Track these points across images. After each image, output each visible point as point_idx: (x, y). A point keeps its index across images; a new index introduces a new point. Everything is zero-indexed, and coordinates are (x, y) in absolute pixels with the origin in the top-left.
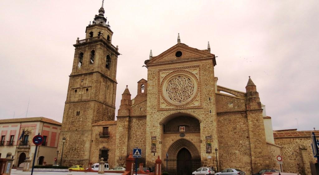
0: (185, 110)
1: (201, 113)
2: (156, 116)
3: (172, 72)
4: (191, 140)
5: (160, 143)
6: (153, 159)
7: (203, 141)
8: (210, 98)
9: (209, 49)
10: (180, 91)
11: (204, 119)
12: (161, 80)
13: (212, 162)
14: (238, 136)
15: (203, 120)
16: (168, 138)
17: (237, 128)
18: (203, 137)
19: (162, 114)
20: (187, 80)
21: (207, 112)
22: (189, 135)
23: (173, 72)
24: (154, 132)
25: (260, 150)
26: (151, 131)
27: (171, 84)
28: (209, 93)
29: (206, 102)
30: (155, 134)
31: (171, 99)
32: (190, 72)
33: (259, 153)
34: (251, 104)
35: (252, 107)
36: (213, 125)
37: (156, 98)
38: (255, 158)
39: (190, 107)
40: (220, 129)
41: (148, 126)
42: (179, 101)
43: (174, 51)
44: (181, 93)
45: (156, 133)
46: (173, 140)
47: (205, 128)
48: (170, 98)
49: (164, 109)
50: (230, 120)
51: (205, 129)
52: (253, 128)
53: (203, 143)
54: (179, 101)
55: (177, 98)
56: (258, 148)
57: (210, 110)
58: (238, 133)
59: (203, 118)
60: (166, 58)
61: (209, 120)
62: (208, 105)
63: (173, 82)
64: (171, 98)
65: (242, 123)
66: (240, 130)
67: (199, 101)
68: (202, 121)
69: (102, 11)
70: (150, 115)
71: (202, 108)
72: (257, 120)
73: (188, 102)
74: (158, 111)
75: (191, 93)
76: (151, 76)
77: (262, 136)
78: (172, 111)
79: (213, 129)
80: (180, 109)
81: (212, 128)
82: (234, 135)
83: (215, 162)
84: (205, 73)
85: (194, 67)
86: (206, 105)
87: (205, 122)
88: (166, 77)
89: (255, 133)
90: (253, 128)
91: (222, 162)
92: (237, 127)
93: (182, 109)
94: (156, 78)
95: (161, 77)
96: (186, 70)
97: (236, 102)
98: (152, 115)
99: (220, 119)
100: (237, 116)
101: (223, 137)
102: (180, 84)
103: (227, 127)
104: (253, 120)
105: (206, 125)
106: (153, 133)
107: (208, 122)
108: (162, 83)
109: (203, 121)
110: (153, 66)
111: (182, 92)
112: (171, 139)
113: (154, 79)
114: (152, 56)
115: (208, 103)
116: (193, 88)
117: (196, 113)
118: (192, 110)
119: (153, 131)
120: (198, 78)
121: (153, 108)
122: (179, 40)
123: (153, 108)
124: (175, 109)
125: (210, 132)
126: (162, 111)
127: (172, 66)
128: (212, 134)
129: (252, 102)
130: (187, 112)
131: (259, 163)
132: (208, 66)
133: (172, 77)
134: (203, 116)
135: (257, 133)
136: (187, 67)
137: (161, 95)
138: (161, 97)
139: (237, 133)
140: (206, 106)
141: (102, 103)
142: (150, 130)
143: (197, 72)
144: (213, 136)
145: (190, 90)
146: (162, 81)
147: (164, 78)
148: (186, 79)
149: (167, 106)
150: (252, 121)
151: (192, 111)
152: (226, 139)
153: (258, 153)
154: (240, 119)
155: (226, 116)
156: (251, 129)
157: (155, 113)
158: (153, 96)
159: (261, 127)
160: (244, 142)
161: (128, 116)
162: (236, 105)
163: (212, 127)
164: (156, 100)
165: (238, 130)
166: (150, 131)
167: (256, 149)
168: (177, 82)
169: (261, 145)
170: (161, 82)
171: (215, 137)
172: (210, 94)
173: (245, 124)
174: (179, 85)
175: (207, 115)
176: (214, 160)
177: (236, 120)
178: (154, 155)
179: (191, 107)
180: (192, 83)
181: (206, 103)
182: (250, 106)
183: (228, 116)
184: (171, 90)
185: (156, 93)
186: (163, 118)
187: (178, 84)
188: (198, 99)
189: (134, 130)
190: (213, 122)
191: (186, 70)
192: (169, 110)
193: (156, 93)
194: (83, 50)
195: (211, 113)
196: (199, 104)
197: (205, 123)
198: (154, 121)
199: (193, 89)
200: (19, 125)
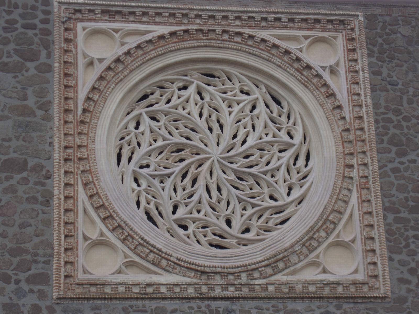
3: (162, 37)
10: (217, 171)
20: (261, 107)
23: (173, 34)
27: (153, 118)
29: (404, 257)
31: (150, 218)
32: (287, 52)
39: (299, 288)
42: (211, 237)
48: (147, 214)
49: (108, 290)
54: (211, 237)
55: (195, 215)
63: (162, 106)
64: (155, 213)
67: (358, 246)
73: (280, 247)
75: (296, 194)
80: (232, 291)
84: (385, 72)
85: (317, 21)
86: (407, 276)
88: (118, 60)
93: (245, 291)
95: (81, 62)
102: (216, 126)
108: (88, 99)
111: (233, 177)
116: (301, 162)
123: (22, 276)
124: (191, 291)
136: (271, 17)
137: (85, 185)
138: (82, 195)
140: (404, 287)
143: (332, 62)
145: (283, 169)
146: (94, 89)
147: (109, 68)
148: (256, 94)
149: (130, 264)
158: (21, 189)
170: (82, 94)
174: (211, 129)
179: (307, 283)
180: (300, 128)
181: (402, 263)
184: (153, 161)
187: (202, 124)
188: (347, 239)
196: (356, 271)
199: (304, 171)
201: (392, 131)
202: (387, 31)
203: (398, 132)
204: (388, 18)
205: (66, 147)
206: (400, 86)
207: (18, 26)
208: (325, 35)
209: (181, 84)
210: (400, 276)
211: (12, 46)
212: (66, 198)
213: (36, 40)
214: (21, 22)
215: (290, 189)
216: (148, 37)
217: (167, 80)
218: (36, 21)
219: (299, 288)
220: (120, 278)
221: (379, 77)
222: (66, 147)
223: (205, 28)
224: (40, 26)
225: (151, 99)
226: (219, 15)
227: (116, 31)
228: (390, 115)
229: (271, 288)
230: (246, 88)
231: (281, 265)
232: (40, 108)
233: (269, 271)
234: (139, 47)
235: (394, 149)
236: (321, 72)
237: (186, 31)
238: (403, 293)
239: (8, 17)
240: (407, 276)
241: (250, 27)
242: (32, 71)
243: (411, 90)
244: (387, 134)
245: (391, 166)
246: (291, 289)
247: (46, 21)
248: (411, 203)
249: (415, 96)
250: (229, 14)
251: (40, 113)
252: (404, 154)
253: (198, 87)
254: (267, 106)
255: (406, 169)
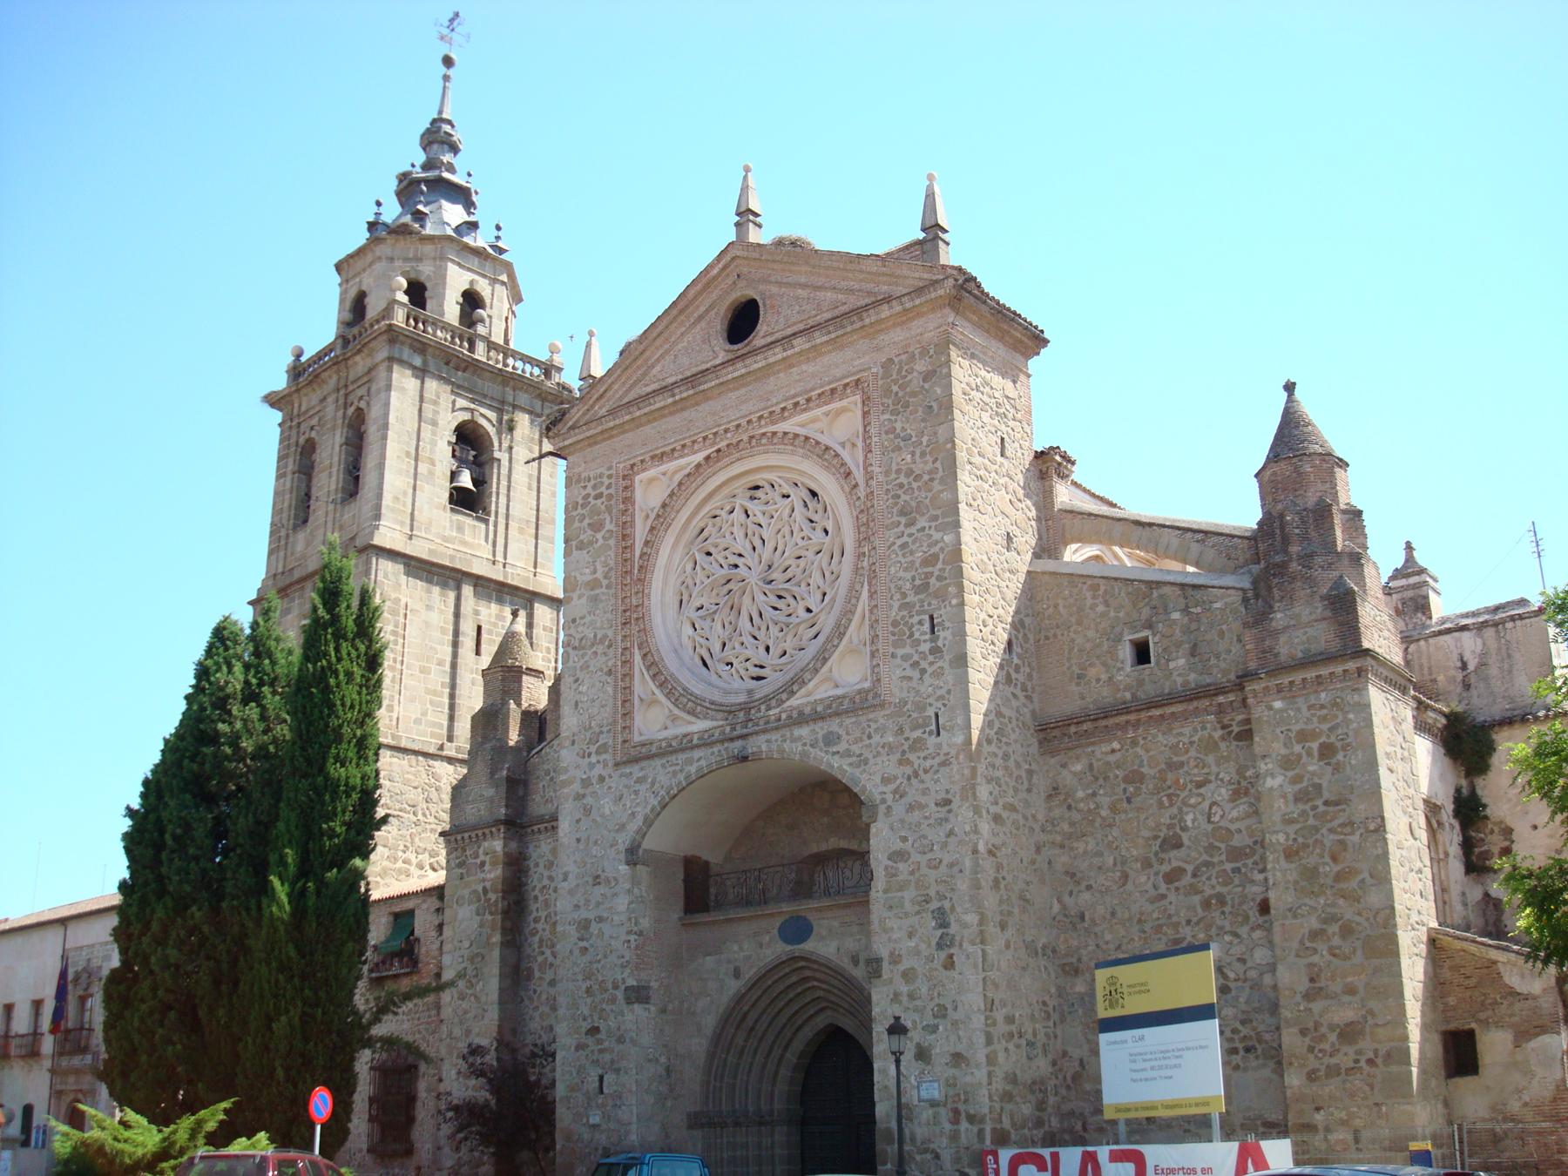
0: (774, 736)
1: (876, 738)
2: (607, 806)
3: (699, 466)
4: (846, 964)
5: (629, 1002)
6: (592, 1121)
7: (885, 965)
8: (932, 618)
9: (933, 231)
11: (892, 787)
12: (640, 532)
13: (948, 1127)
14: (1196, 899)
15: (889, 797)
16: (709, 961)
17: (1185, 837)
18: (885, 931)
19: (643, 788)
21: (917, 734)
22: (836, 924)
23: (708, 458)
24: (600, 919)
25: (1344, 1014)
26: (584, 914)
28: (928, 575)
30: (601, 934)
31: (705, 664)
33: (1340, 1035)
34: (1279, 618)
35: (1283, 639)
36: (951, 833)
37: (610, 673)
38: (1312, 1076)
40: (1064, 859)
41: (565, 879)
43: (711, 307)
44: (769, 613)
45: (607, 929)
46: (737, 974)
47: (898, 856)
50: (1135, 778)
51: (901, 866)
52: (1292, 821)
53: (891, 981)
56: (1337, 987)
57: (931, 712)
58: (1194, 875)
59: (886, 780)
60: (668, 369)
61: (925, 792)
62: (923, 671)
65: (1224, 793)
66: (1211, 849)
68: (882, 808)
69: (437, 138)
70: (579, 797)
71: (882, 706)
72: (1327, 751)
74: (617, 765)
76: (583, 517)
77: (1369, 881)
78: (697, 754)
79: (951, 865)
81: (947, 860)
82: (1163, 897)
83: (964, 1125)
84: (898, 426)
85: (833, 391)
86: (909, 672)
87: (899, 809)
88: (664, 506)
89: (1311, 861)
90: (1292, 821)
91: (1079, 1127)
92: (1184, 829)
94: (609, 526)
96: (782, 427)
97: (1176, 616)
98: (589, 800)
99: (1067, 778)
100: (1187, 731)
101: (1082, 917)
103: (1115, 832)
104: (1299, 756)
105: (904, 839)
106: (594, 928)
107: (921, 807)
108: (643, 555)
109: (889, 808)
110: (592, 441)
112: (729, 962)
113: (599, 536)
114: (590, 376)
115: (923, 655)
117: (842, 747)
118: (821, 729)
119: (591, 916)
120: (859, 475)
121: (593, 749)
122: (746, 216)
125: (932, 893)
126: (644, 763)
127: (702, 417)
128: (947, 904)
129: (1290, 598)
130: (786, 746)
131: (1344, 1123)
132: (921, 366)
133: (710, 495)
134: (888, 764)
135: (1327, 859)
138: (638, 658)
139: (1187, 880)
141: (426, 755)
142: (577, 907)
144: (952, 919)
145: (817, 576)
147: (658, 516)
149: (674, 719)
150: (1287, 763)
151: (820, 736)
152: (1108, 937)
153: (1333, 1037)
154: (1210, 759)
155: (1105, 748)
156: (1281, 838)
157: (602, 779)
159: (1360, 809)
160: (1237, 950)
161: (497, 822)
162: (1178, 645)
163: (944, 845)
164: (610, 690)
165: (1193, 854)
166: (576, 915)
167: (1316, 1007)
168: (739, 534)
169: (1358, 958)
171: (965, 926)
172: (933, 581)
173: (1246, 793)
175: (912, 757)
176: (956, 1112)
177: (1182, 764)
178: (601, 1092)
182: (1275, 634)
183: (1116, 745)
185: (610, 633)
186: (648, 810)
189: (543, 914)
190: (954, 806)
191: (782, 427)
192: (685, 745)
193: (610, 633)
194: (314, 421)
195: (938, 734)
197: (902, 821)
198: (596, 843)
200: (53, 939)
201: (904, 497)
202: (904, 373)
203: (907, 498)
204: (904, 357)
205: (625, 611)
206: (914, 439)
207: (590, 499)
208: (845, 403)
209: (728, 508)
210: (904, 674)
211: (587, 521)
212: (624, 662)
213: (603, 507)
214: (593, 494)
215: (824, 594)
216: (687, 471)
217: (716, 508)
218: (603, 489)
219: (807, 710)
220: (665, 734)
221: (892, 436)
222: (625, 611)
223: (734, 441)
224: (606, 493)
225: (705, 533)
226: (743, 422)
227: (664, 474)
228: (902, 479)
229: (784, 716)
230: (785, 492)
231: (795, 688)
232: (605, 577)
233: (784, 696)
234: (680, 484)
235: (903, 520)
236: (839, 449)
237: (719, 451)
238: (905, 694)
239: (584, 493)
240: (909, 672)
241: (773, 423)
242: (601, 541)
243: (925, 440)
244: (897, 504)
245: (899, 542)
246: (801, 714)
247: (609, 487)
248: (918, 582)
249: (928, 446)
250: (752, 417)
251: (605, 582)
252: (911, 524)
253: (742, 506)
254: (806, 505)
255: (914, 542)
